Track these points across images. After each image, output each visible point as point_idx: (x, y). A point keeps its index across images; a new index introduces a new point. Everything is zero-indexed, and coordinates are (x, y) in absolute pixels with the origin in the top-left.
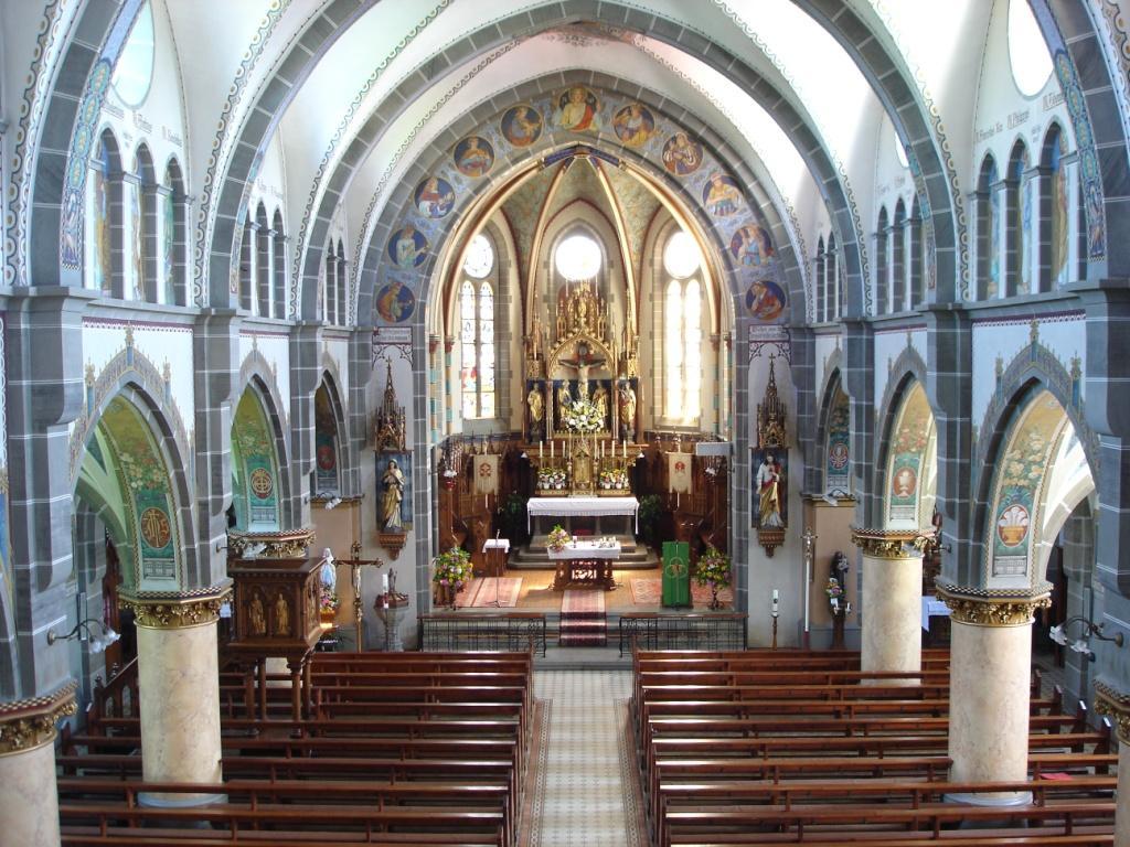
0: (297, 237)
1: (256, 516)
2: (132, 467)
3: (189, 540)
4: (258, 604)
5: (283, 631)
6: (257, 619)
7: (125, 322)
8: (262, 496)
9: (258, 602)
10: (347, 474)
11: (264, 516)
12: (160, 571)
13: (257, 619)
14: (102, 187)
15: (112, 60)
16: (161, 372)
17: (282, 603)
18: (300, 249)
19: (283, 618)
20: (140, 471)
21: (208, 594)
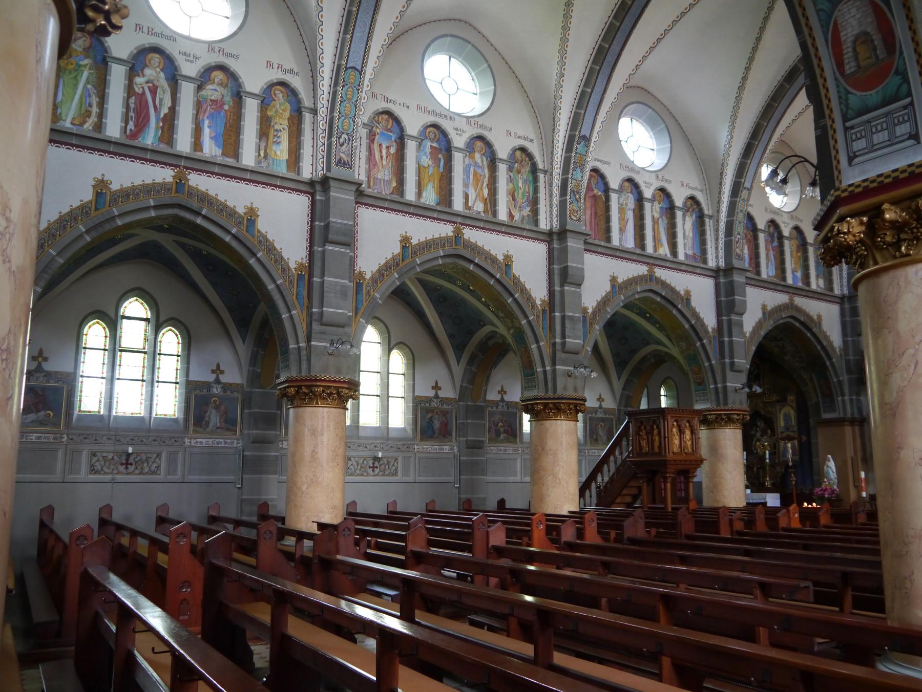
0: (716, 214)
1: (698, 398)
2: (506, 320)
3: (544, 366)
4: (643, 433)
5: (656, 450)
6: (644, 443)
7: (455, 223)
8: (700, 384)
9: (644, 431)
10: (843, 401)
11: (702, 398)
12: (530, 384)
13: (644, 443)
14: (440, 156)
15: (588, 136)
16: (500, 258)
17: (656, 431)
18: (718, 221)
19: (656, 444)
20: (509, 321)
21: (554, 399)
